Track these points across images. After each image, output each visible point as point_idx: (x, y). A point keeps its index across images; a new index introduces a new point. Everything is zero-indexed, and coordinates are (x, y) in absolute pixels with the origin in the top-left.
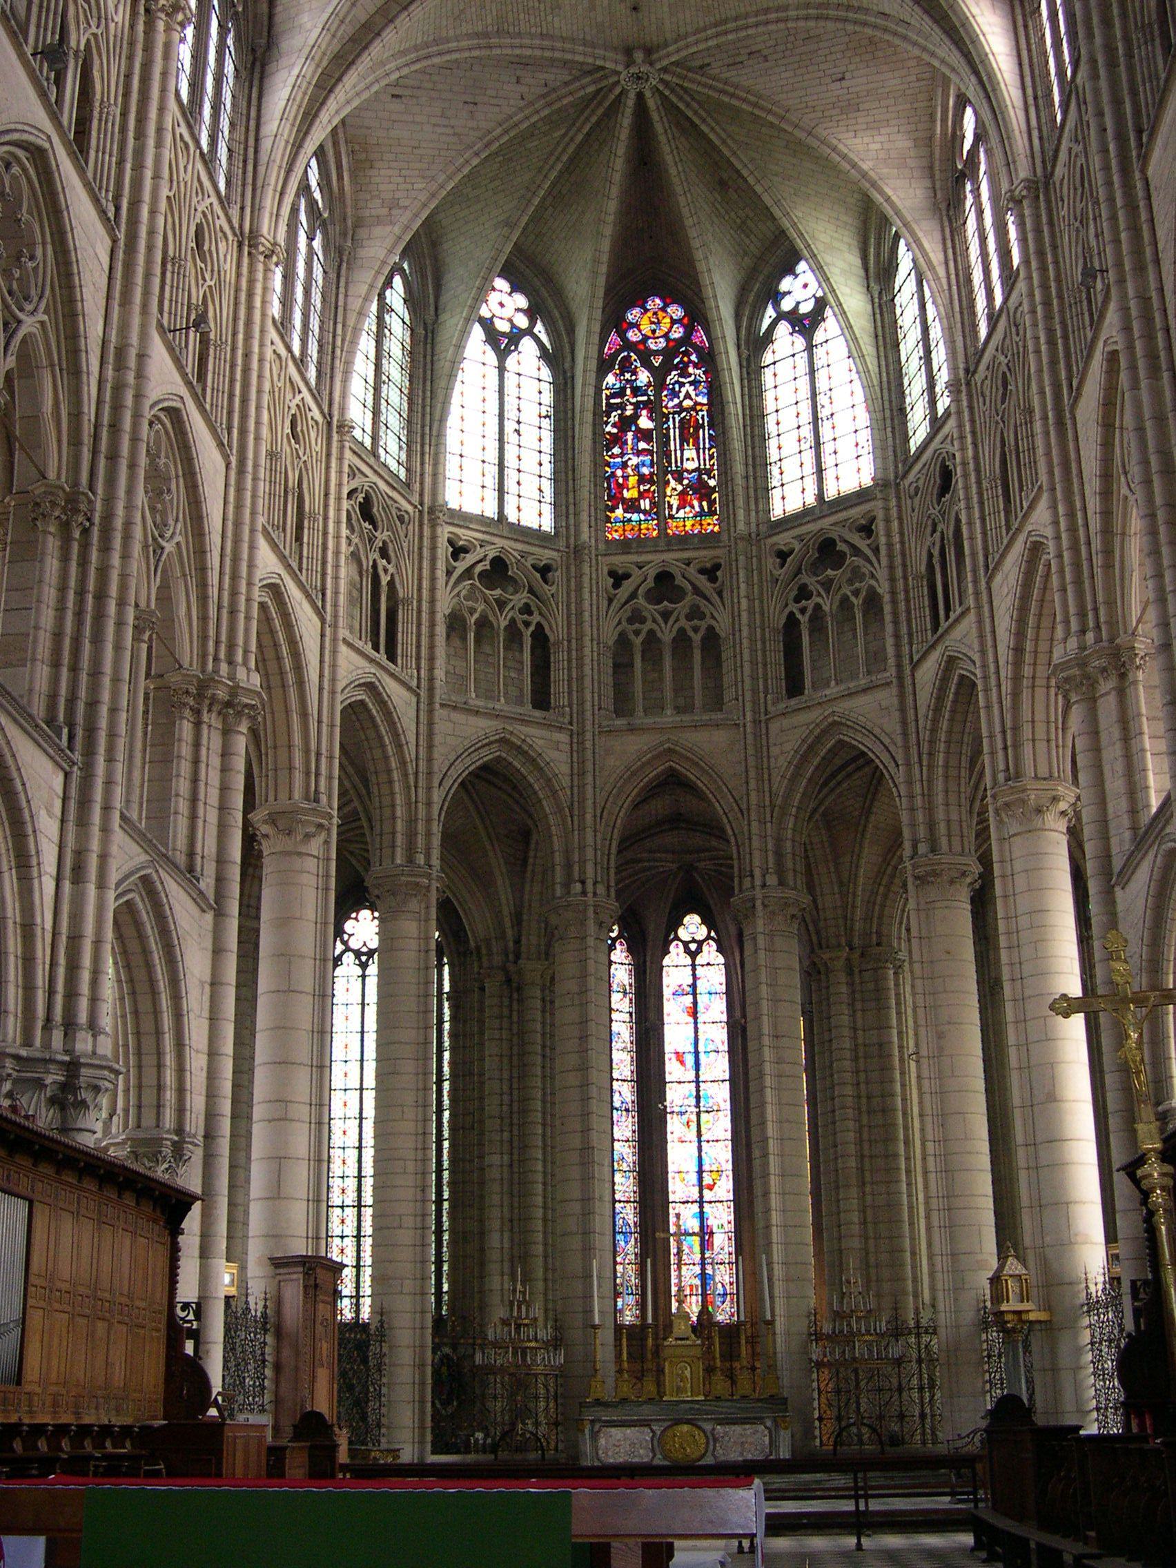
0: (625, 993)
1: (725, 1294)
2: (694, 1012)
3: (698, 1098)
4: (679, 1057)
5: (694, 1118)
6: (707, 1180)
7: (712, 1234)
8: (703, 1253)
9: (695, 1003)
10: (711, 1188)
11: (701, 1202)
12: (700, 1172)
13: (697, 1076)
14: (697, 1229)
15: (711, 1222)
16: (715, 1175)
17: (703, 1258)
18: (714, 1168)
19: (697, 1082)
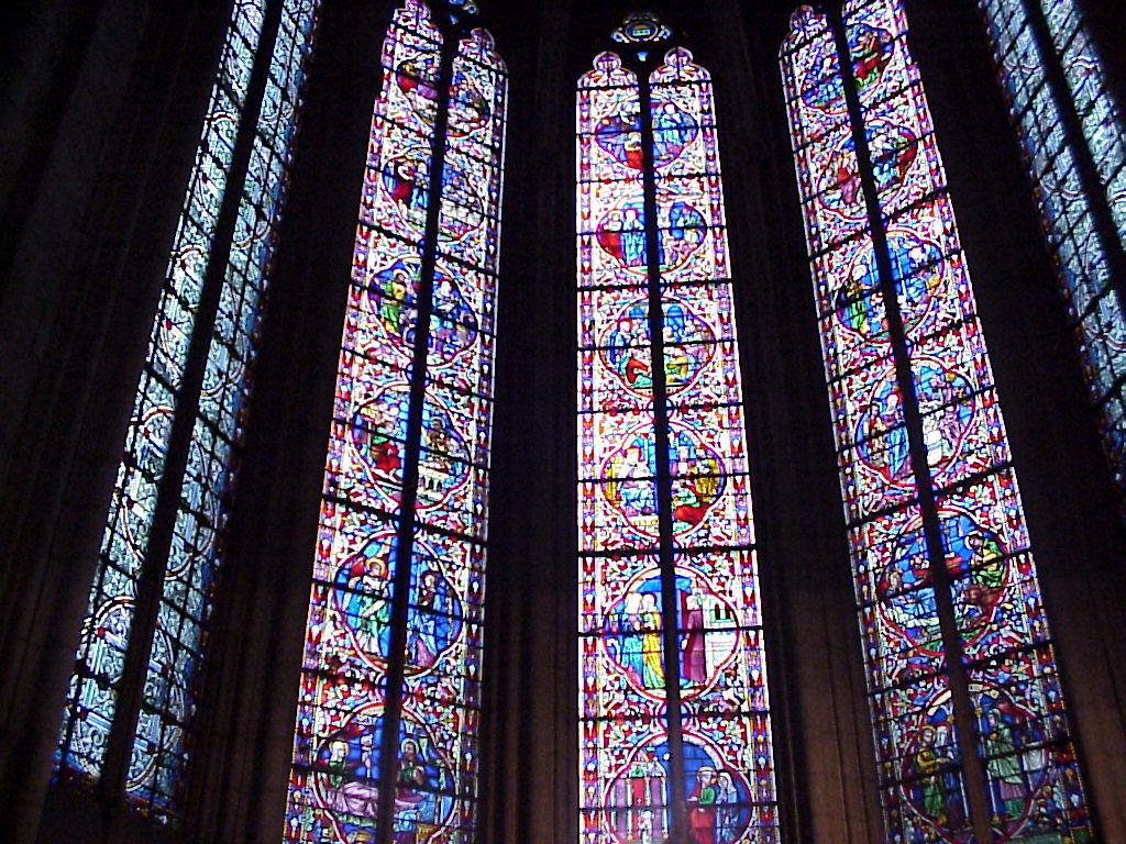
0: (483, 112)
1: (744, 804)
2: (645, 161)
3: (656, 319)
4: (611, 242)
5: (644, 357)
6: (682, 496)
7: (700, 632)
8: (671, 685)
9: (647, 143)
10: (693, 516)
11: (666, 552)
12: (663, 479)
13: (654, 274)
14: (654, 621)
15: (701, 602)
16: (702, 487)
17: (673, 698)
18: (700, 467)
19: (654, 285)
